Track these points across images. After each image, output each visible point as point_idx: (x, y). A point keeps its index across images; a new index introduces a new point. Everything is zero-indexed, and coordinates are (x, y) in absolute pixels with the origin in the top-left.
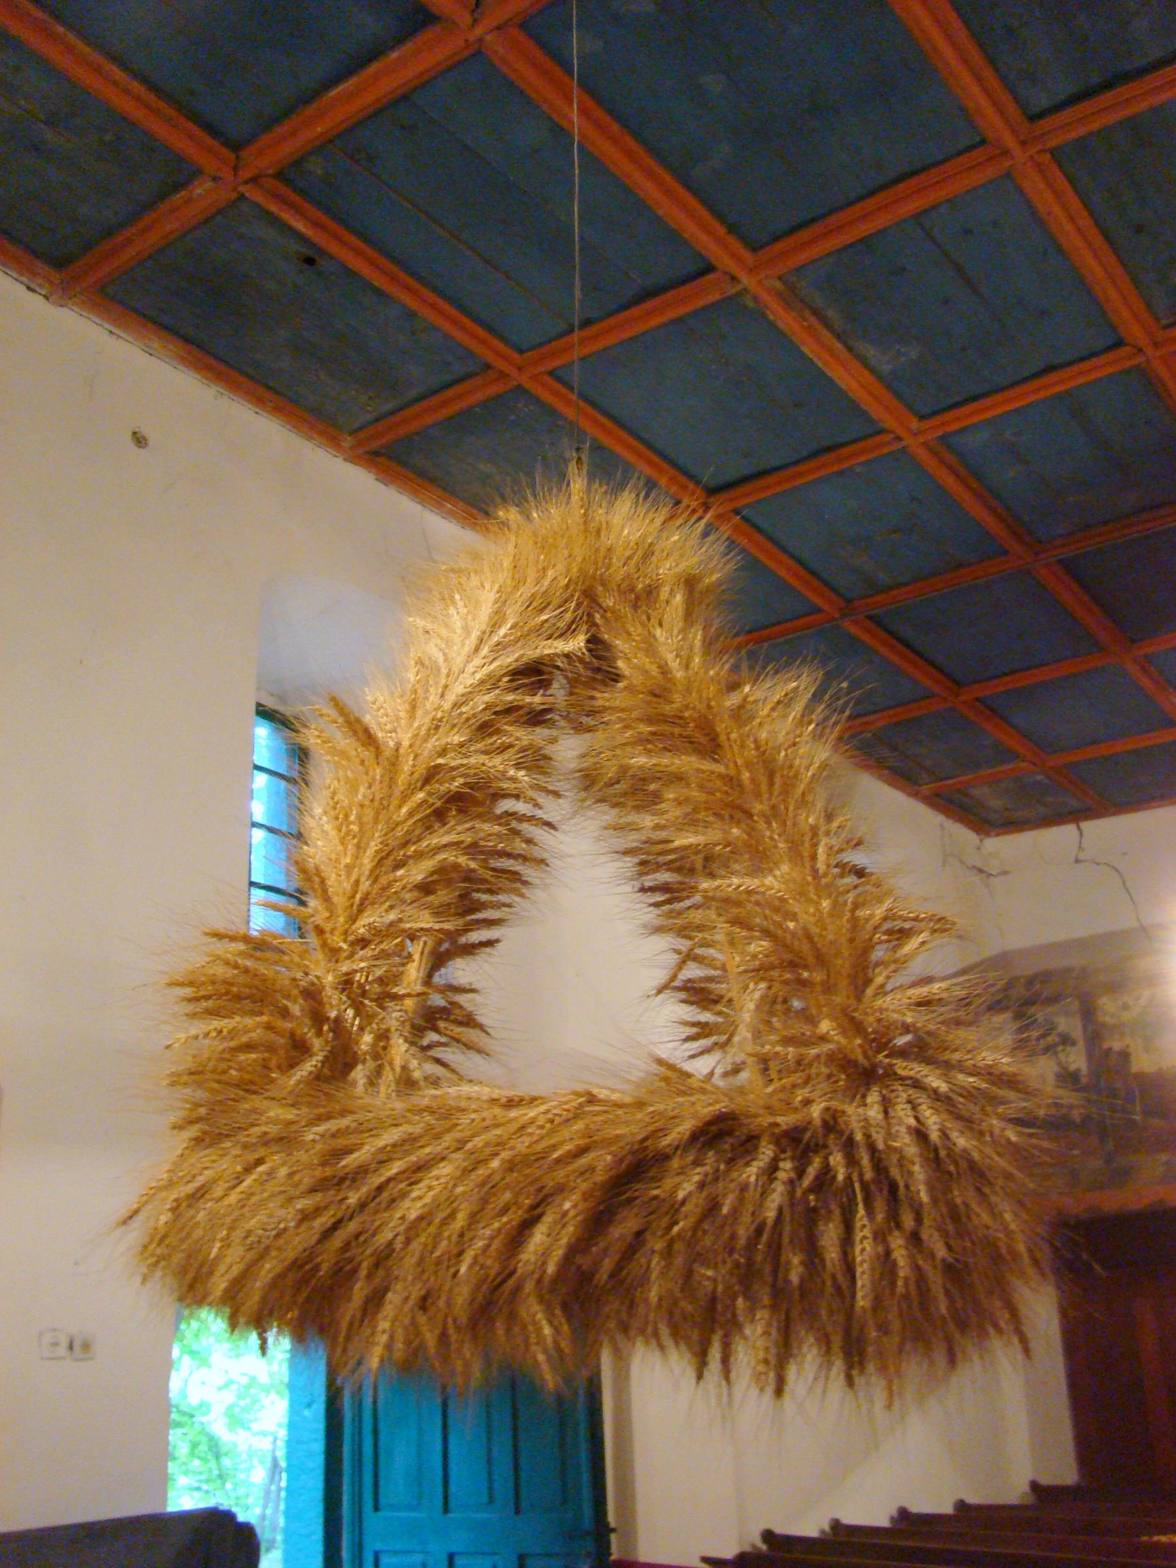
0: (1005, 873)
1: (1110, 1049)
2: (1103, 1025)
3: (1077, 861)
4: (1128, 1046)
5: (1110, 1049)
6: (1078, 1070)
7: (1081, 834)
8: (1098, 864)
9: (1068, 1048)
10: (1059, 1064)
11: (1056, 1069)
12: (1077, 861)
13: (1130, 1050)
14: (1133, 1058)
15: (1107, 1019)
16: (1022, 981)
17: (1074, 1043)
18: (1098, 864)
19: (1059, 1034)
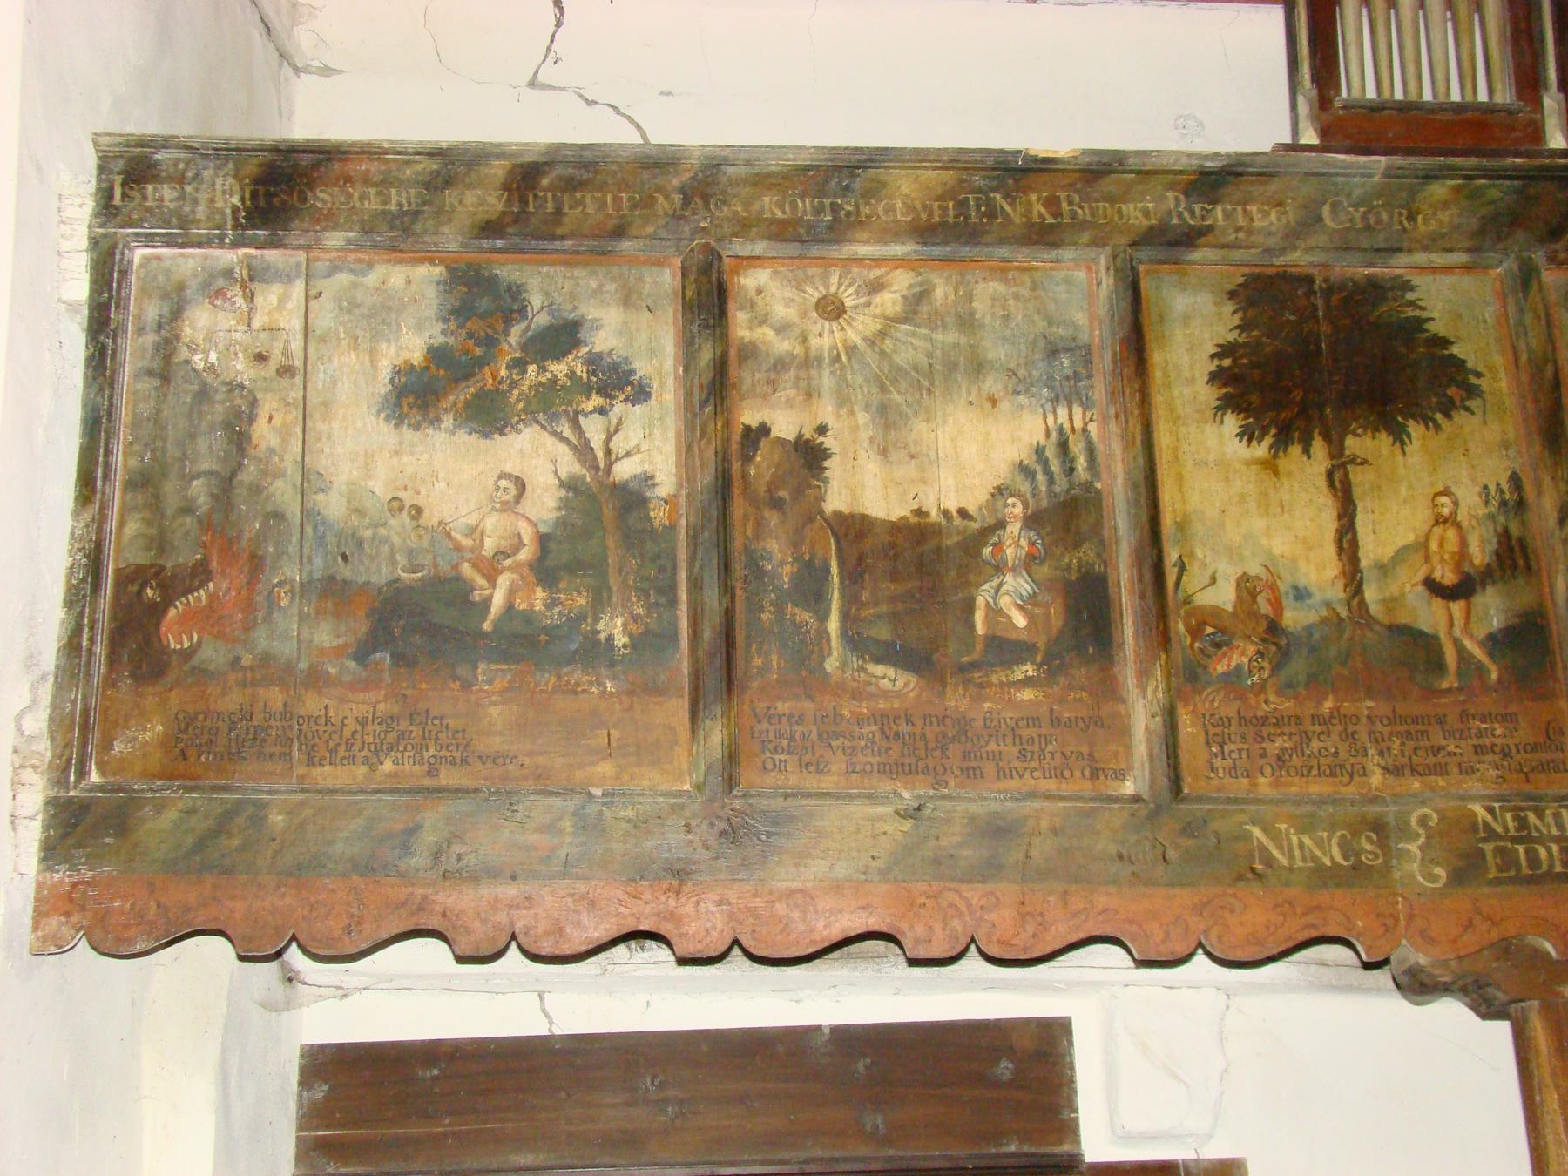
0: (326, 71)
1: (764, 430)
2: (749, 352)
3: (532, 84)
4: (822, 430)
5: (764, 430)
6: (647, 479)
7: (559, 24)
8: (591, 103)
9: (619, 408)
10: (583, 450)
11: (569, 465)
12: (532, 84)
13: (828, 442)
14: (833, 466)
15: (766, 334)
16: (498, 170)
17: (641, 394)
18: (591, 103)
19: (593, 361)
